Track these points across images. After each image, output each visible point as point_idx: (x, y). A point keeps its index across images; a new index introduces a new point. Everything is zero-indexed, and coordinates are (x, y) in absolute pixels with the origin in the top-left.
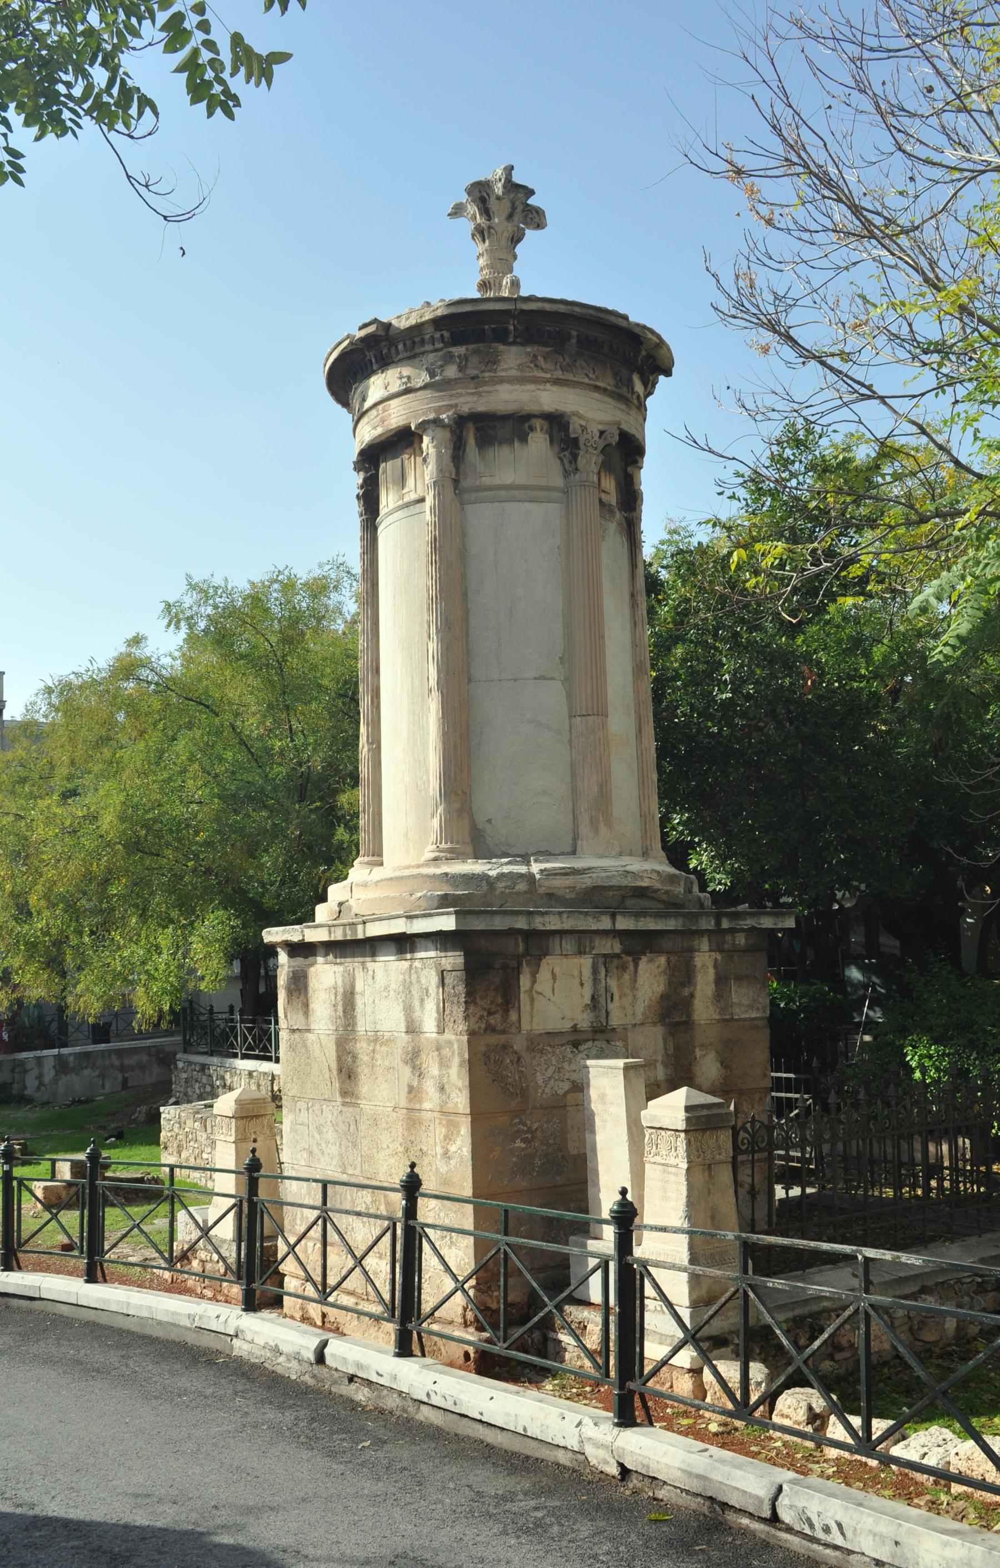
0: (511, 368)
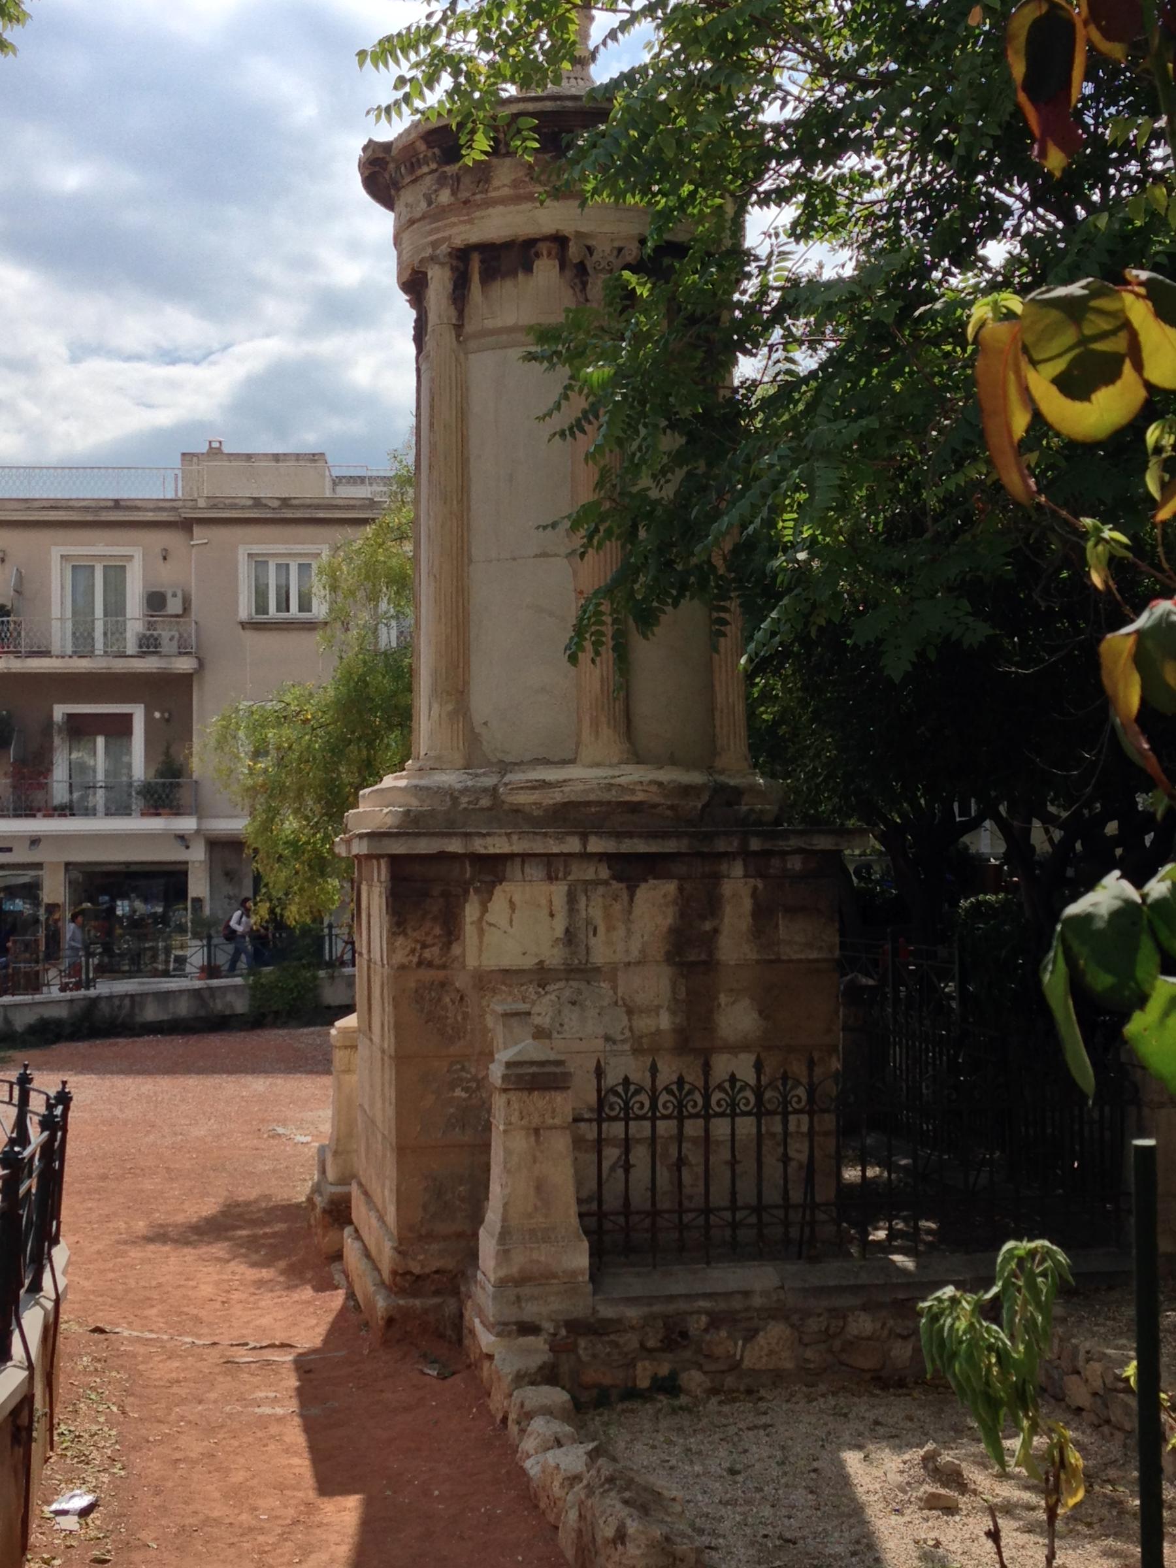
0: (504, 186)
